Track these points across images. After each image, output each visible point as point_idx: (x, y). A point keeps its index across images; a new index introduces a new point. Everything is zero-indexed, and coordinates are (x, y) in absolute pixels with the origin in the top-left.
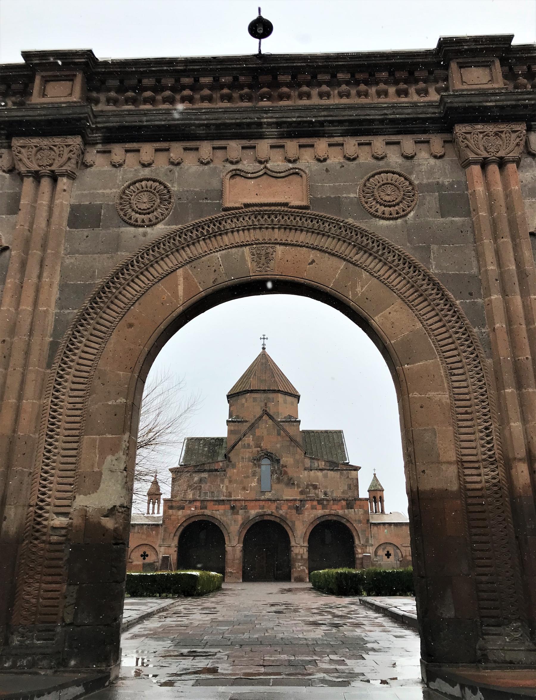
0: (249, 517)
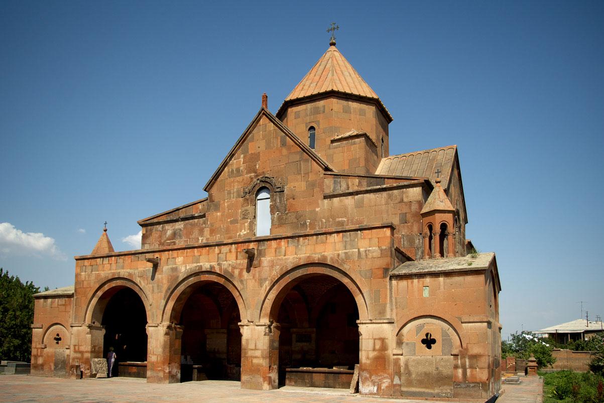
0: (178, 277)
